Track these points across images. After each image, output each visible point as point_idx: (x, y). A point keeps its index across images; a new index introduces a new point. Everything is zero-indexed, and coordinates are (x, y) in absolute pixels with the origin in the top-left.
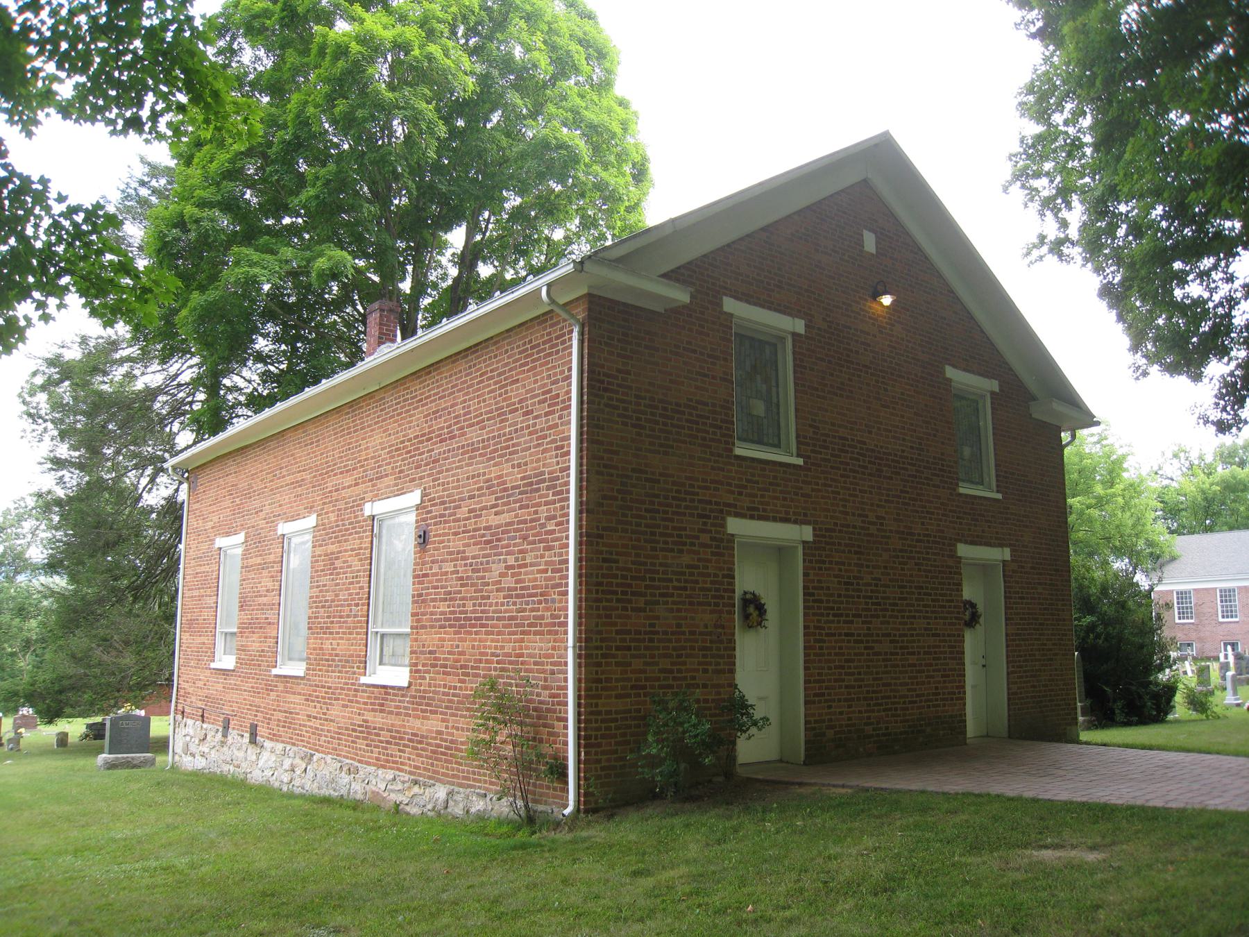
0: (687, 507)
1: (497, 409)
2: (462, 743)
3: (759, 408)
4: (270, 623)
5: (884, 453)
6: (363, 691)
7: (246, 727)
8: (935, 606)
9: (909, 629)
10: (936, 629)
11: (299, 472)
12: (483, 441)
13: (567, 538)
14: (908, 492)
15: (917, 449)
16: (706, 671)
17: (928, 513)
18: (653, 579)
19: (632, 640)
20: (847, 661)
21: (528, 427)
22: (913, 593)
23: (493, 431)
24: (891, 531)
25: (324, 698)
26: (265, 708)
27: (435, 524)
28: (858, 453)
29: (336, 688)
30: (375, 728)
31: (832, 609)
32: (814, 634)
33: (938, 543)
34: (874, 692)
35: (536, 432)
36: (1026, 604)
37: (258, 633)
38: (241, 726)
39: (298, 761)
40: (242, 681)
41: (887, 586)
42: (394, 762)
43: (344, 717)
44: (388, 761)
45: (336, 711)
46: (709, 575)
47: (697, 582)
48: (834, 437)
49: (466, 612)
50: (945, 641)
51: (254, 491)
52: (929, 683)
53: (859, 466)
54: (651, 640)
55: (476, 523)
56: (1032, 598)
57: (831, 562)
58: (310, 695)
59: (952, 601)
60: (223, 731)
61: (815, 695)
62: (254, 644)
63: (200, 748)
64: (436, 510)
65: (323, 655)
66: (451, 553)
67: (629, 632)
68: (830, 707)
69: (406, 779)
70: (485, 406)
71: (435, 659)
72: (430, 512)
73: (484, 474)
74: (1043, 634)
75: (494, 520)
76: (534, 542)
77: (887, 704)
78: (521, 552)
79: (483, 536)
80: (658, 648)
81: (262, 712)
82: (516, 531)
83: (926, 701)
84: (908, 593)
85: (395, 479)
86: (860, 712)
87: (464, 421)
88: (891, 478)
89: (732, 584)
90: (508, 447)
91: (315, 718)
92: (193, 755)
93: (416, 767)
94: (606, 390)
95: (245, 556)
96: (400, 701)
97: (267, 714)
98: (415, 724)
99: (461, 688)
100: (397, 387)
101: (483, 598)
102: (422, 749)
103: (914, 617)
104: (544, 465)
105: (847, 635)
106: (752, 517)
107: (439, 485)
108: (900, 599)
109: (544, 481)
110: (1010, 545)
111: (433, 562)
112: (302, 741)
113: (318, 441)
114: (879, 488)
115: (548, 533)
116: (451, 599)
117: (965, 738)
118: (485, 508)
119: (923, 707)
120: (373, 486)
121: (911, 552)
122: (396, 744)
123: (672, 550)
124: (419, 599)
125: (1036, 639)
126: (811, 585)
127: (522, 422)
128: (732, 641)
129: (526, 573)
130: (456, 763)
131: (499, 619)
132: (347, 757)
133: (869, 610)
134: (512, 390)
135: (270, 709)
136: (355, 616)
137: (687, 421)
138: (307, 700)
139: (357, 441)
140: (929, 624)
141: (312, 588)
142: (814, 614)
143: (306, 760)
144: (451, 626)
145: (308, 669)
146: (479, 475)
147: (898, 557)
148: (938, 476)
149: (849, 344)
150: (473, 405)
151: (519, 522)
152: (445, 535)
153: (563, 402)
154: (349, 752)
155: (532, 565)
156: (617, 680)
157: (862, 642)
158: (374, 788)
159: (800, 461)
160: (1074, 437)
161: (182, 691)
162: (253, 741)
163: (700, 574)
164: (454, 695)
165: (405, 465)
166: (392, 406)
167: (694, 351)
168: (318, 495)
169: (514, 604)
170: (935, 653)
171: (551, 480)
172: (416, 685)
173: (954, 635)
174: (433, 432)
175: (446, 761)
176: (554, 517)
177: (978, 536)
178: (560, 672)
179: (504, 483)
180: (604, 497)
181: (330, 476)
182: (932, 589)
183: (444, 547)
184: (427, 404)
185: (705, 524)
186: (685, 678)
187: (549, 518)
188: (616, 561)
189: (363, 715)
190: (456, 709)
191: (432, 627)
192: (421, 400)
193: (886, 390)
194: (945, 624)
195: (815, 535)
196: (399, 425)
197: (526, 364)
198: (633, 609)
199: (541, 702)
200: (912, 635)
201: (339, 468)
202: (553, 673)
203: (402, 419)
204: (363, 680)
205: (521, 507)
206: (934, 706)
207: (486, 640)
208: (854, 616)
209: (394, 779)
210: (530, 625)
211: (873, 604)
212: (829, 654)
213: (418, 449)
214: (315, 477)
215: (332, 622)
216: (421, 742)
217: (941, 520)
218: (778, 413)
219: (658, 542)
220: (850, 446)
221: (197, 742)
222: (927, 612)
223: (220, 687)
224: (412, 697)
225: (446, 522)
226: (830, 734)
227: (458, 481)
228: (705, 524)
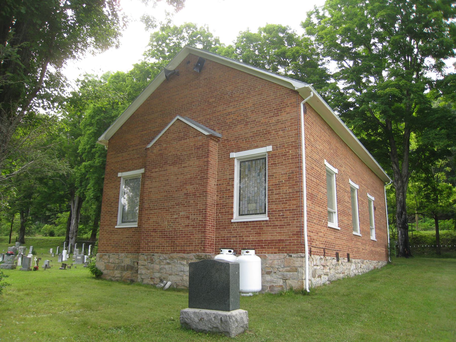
7: (345, 255)
26: (351, 247)
40: (342, 236)
81: (350, 248)
92: (320, 276)
135: (353, 247)
162: (349, 260)
223: (333, 237)
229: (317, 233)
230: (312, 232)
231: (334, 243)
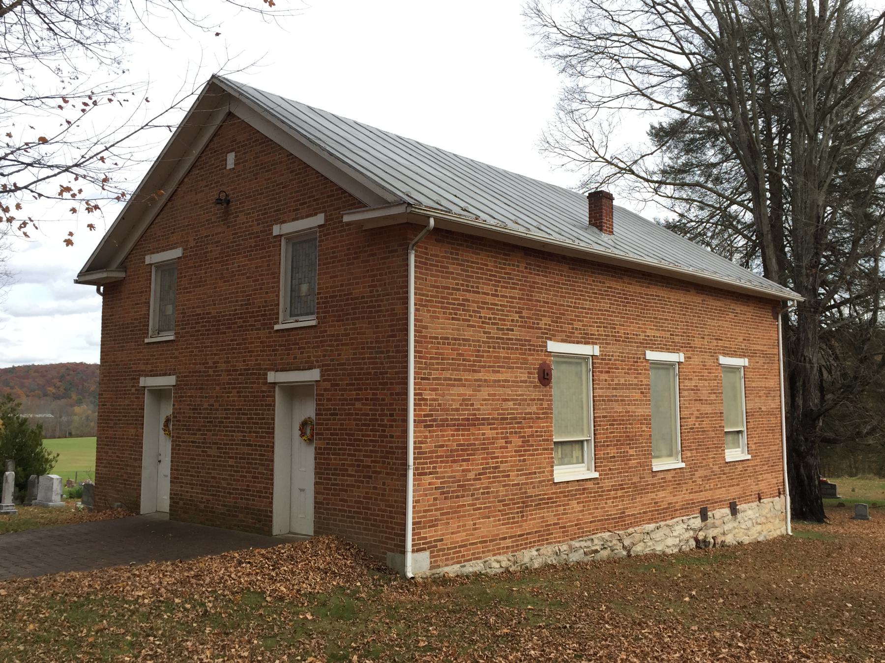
8: (249, 423)
9: (230, 440)
10: (250, 441)
22: (235, 414)
24: (222, 371)
33: (255, 374)
34: (206, 481)
41: (217, 410)
50: (257, 450)
52: (242, 481)
57: (186, 397)
59: (264, 419)
68: (182, 487)
83: (240, 494)
84: (231, 414)
103: (234, 431)
105: (193, 442)
106: (151, 376)
108: (225, 418)
121: (235, 384)
140: (244, 436)
142: (177, 429)
157: (200, 447)
170: (248, 459)
173: (263, 446)
182: (249, 410)
194: (257, 437)
200: (232, 444)
208: (197, 430)
211: (208, 422)
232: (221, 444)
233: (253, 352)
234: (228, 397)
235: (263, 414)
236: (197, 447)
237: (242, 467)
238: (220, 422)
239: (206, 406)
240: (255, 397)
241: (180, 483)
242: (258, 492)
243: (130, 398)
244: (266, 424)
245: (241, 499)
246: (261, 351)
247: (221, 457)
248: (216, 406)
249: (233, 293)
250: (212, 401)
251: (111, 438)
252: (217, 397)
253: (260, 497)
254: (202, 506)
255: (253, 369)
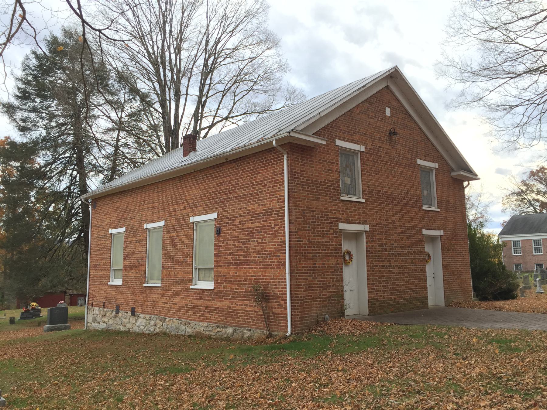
0: (325, 220)
1: (251, 183)
2: (240, 310)
3: (348, 181)
4: (141, 265)
5: (394, 196)
6: (191, 292)
8: (414, 254)
9: (405, 263)
10: (415, 263)
11: (154, 203)
12: (245, 195)
13: (284, 233)
14: (403, 210)
15: (407, 193)
16: (333, 281)
17: (411, 218)
18: (314, 247)
19: (308, 270)
20: (383, 276)
21: (265, 191)
22: (406, 249)
23: (249, 191)
24: (397, 226)
25: (172, 295)
27: (224, 226)
28: (385, 196)
29: (178, 291)
30: (198, 306)
31: (377, 256)
32: (370, 266)
33: (415, 229)
35: (269, 193)
36: (451, 252)
37: (134, 269)
38: (126, 309)
39: (158, 321)
40: (126, 290)
42: (207, 319)
43: (182, 302)
44: (204, 319)
45: (177, 300)
46: (333, 245)
47: (329, 248)
48: (376, 190)
49: (240, 260)
50: (419, 268)
51: (130, 210)
52: (413, 284)
53: (385, 201)
54: (314, 270)
55: (243, 226)
56: (453, 250)
57: (376, 239)
58: (164, 294)
59: (421, 252)
60: (116, 311)
61: (372, 289)
62: (133, 274)
63: (103, 319)
64: (224, 221)
65: (170, 277)
66: (233, 237)
67: (307, 267)
68: (377, 294)
69: (214, 325)
70: (245, 182)
71: (226, 278)
72: (222, 221)
73: (246, 208)
74: (457, 265)
75: (251, 225)
76: (269, 234)
77: (398, 292)
78: (264, 238)
79: (247, 231)
80: (317, 273)
81: (138, 302)
82: (261, 230)
83: (412, 291)
84: (404, 249)
85: (204, 208)
86: (388, 295)
87: (236, 187)
88: (397, 205)
89: (341, 248)
90: (257, 198)
91: (167, 303)
92: (99, 323)
93: (218, 321)
94: (297, 178)
95: (126, 236)
96: (209, 295)
97: (141, 303)
98: (217, 304)
99: (238, 289)
100: (203, 171)
101: (247, 254)
102: (221, 313)
103: (407, 259)
104: (273, 206)
105: (382, 266)
106: (347, 223)
107: (225, 211)
108: (401, 252)
109: (273, 211)
110: (443, 229)
111: (224, 241)
112: (161, 313)
113: (164, 191)
114: (392, 209)
115: (275, 231)
116: (232, 255)
117: (428, 306)
118: (247, 221)
119: (411, 294)
120: (193, 210)
121: (405, 233)
122: (208, 312)
123: (321, 236)
124: (217, 255)
125: (454, 267)
126: (369, 247)
127: (262, 189)
128: (342, 269)
129: (266, 246)
130: (237, 318)
131: (255, 263)
132: (184, 319)
133: (390, 256)
134: (257, 177)
136: (186, 262)
137: (325, 188)
138: (163, 296)
139: (184, 192)
141: (163, 250)
142: (370, 258)
143: (163, 321)
144: (233, 265)
145: (162, 283)
146: (244, 208)
147: (400, 235)
148: (414, 203)
149: (381, 154)
150: (240, 181)
151: (262, 227)
152: (228, 230)
153: (280, 182)
154: (185, 316)
155: (269, 242)
156: (304, 285)
157: (387, 268)
158: (198, 330)
159: (364, 201)
160: (469, 184)
161: (91, 296)
162: (133, 313)
163: (330, 245)
164: (235, 292)
165: (208, 202)
166: (201, 179)
167: (326, 161)
168: (165, 213)
169: (262, 257)
170: (415, 272)
171: (276, 211)
172: (217, 288)
173: (422, 265)
174: (222, 190)
175: (232, 317)
176: (278, 225)
177: (430, 226)
178: (282, 282)
179: (256, 211)
180: (297, 218)
181: (171, 205)
182: (413, 247)
183: (229, 235)
184: (218, 179)
185: (331, 226)
186: (326, 284)
187: (276, 225)
188: (302, 241)
189: (192, 301)
190: (236, 297)
191: (224, 266)
192: (215, 177)
193: (394, 171)
194: (418, 261)
195: (370, 228)
196: (205, 187)
197: (264, 167)
198: (308, 259)
199: (274, 294)
200: (406, 266)
201: (175, 202)
202: (279, 282)
203: (206, 184)
204: (191, 287)
205: (263, 221)
206: (416, 293)
207: (250, 271)
208: (385, 259)
209: (208, 326)
210: (268, 265)
212: (376, 273)
213: (214, 196)
214: (162, 205)
215: (175, 264)
216: (220, 311)
217: (416, 220)
218: (355, 182)
219: (316, 234)
220: (382, 194)
221: (101, 317)
222: (411, 257)
223: (114, 293)
224: (215, 293)
225: (229, 225)
226: (377, 304)
227: (234, 210)
228: (331, 226)
229: (98, 291)
230: (94, 291)
231: (115, 298)
232: (400, 266)
233: (413, 218)
234: (402, 240)
235: (420, 250)
236: (385, 268)
237: (412, 277)
238: (398, 254)
239: (389, 244)
240: (416, 241)
241: (376, 291)
242: (421, 288)
243: (329, 237)
244: (422, 254)
245: (413, 293)
246: (417, 218)
247: (401, 273)
248: (396, 244)
249: (399, 185)
250: (393, 242)
251: (310, 267)
252: (396, 240)
253: (422, 291)
254: (391, 302)
255: (414, 227)
